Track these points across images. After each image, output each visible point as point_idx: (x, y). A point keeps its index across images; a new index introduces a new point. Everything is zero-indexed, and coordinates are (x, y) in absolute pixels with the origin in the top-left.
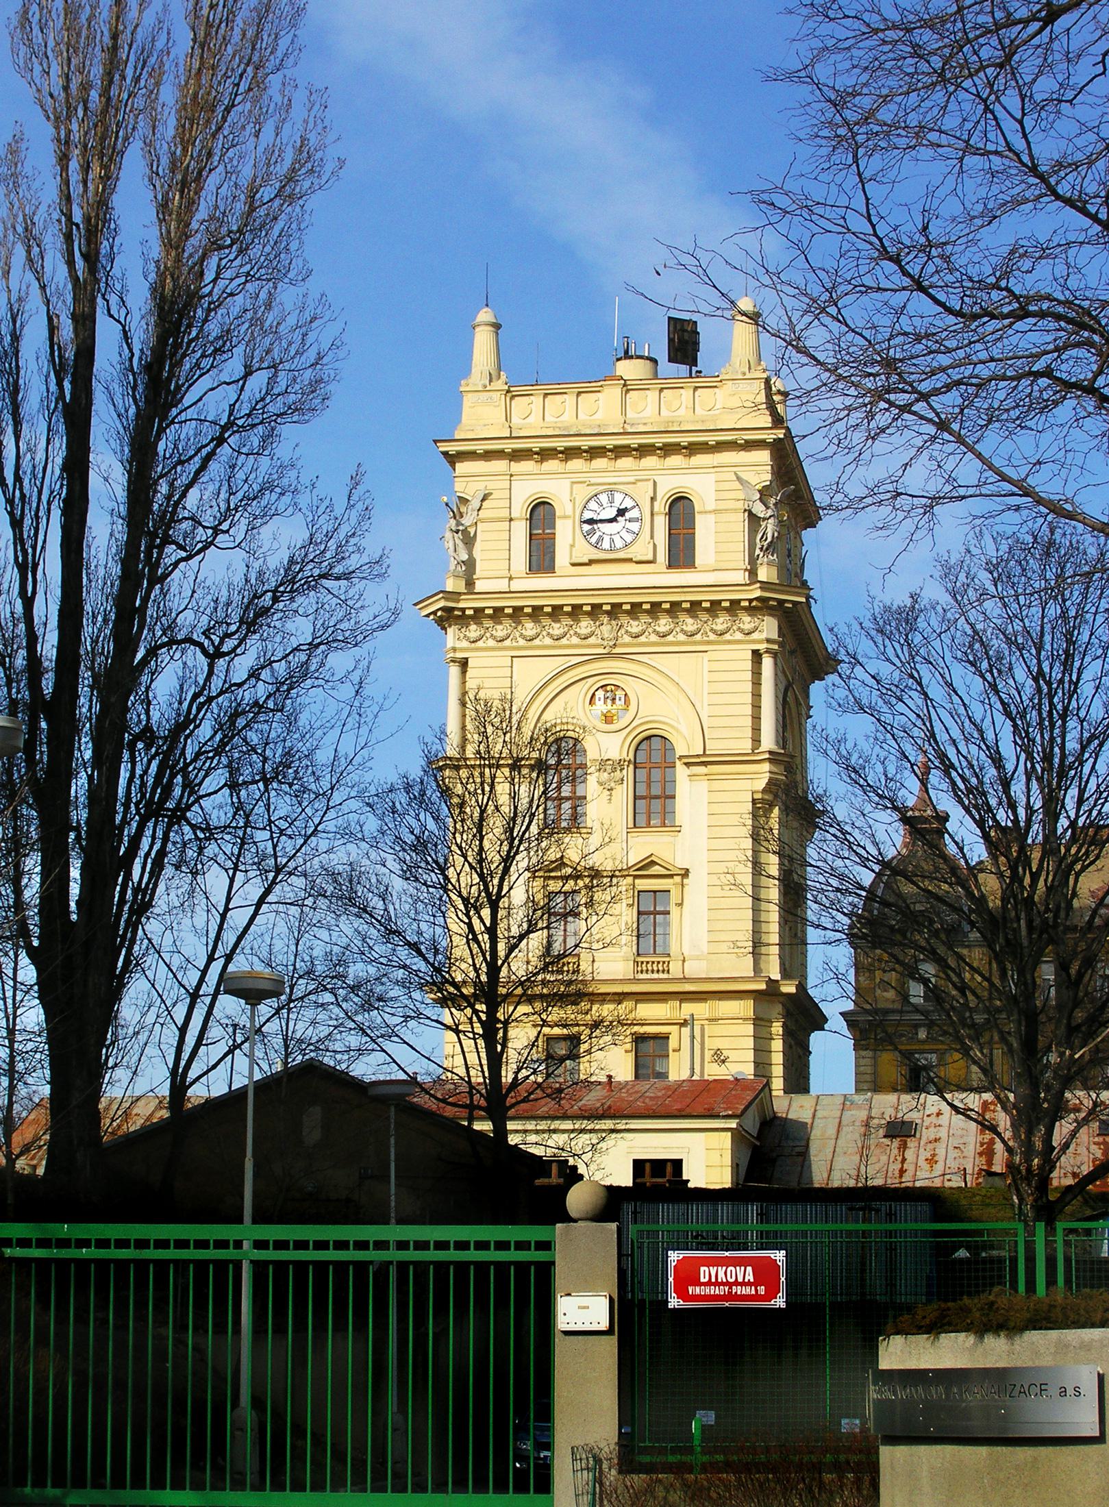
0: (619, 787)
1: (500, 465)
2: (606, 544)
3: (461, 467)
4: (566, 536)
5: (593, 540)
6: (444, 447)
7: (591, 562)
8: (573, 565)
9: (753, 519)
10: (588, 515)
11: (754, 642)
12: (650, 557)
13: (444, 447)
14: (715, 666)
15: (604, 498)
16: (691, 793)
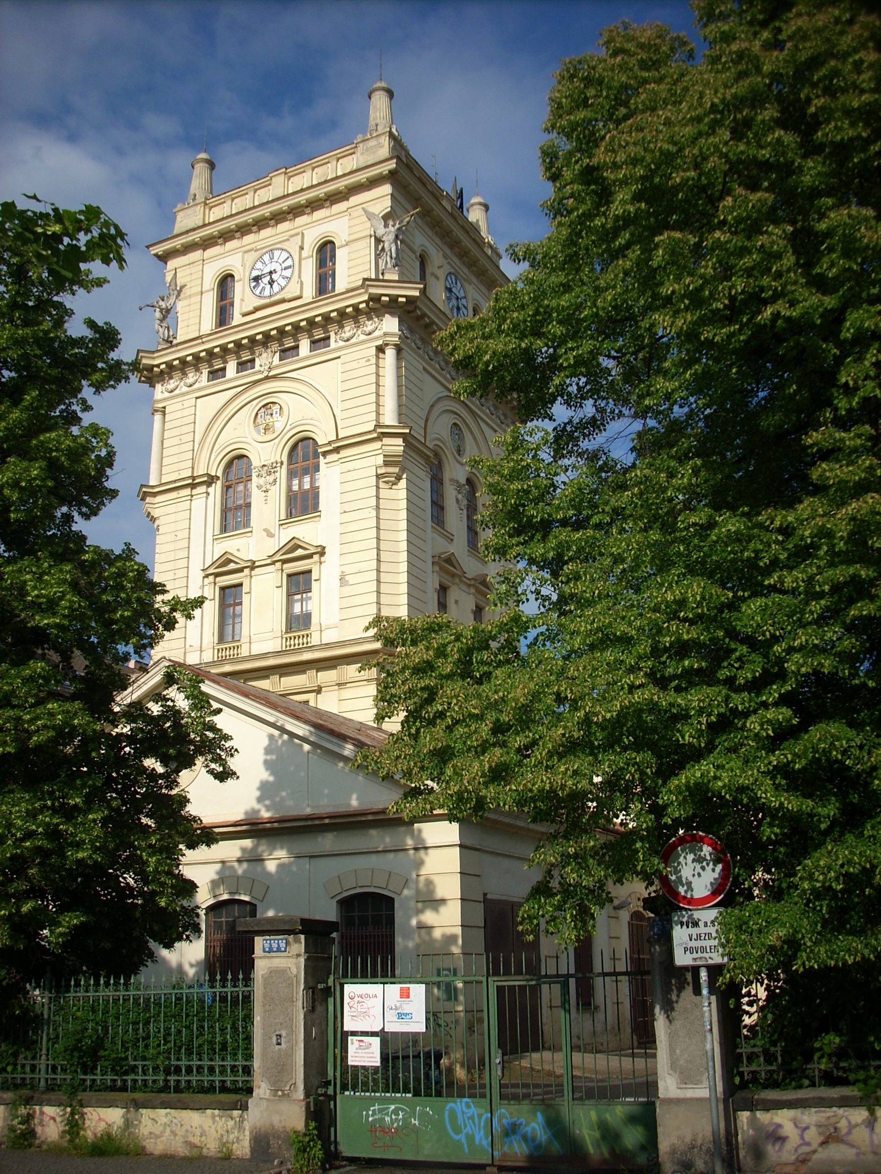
0: (273, 488)
1: (197, 255)
2: (267, 293)
3: (172, 264)
4: (244, 298)
5: (258, 292)
6: (155, 250)
7: (257, 309)
8: (244, 315)
9: (378, 241)
10: (255, 273)
11: (377, 338)
12: (298, 293)
13: (155, 250)
14: (349, 366)
15: (266, 258)
16: (330, 477)
